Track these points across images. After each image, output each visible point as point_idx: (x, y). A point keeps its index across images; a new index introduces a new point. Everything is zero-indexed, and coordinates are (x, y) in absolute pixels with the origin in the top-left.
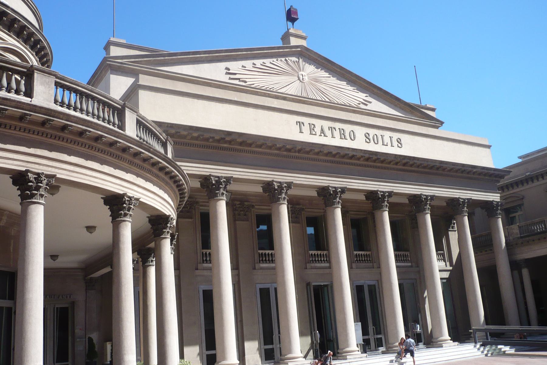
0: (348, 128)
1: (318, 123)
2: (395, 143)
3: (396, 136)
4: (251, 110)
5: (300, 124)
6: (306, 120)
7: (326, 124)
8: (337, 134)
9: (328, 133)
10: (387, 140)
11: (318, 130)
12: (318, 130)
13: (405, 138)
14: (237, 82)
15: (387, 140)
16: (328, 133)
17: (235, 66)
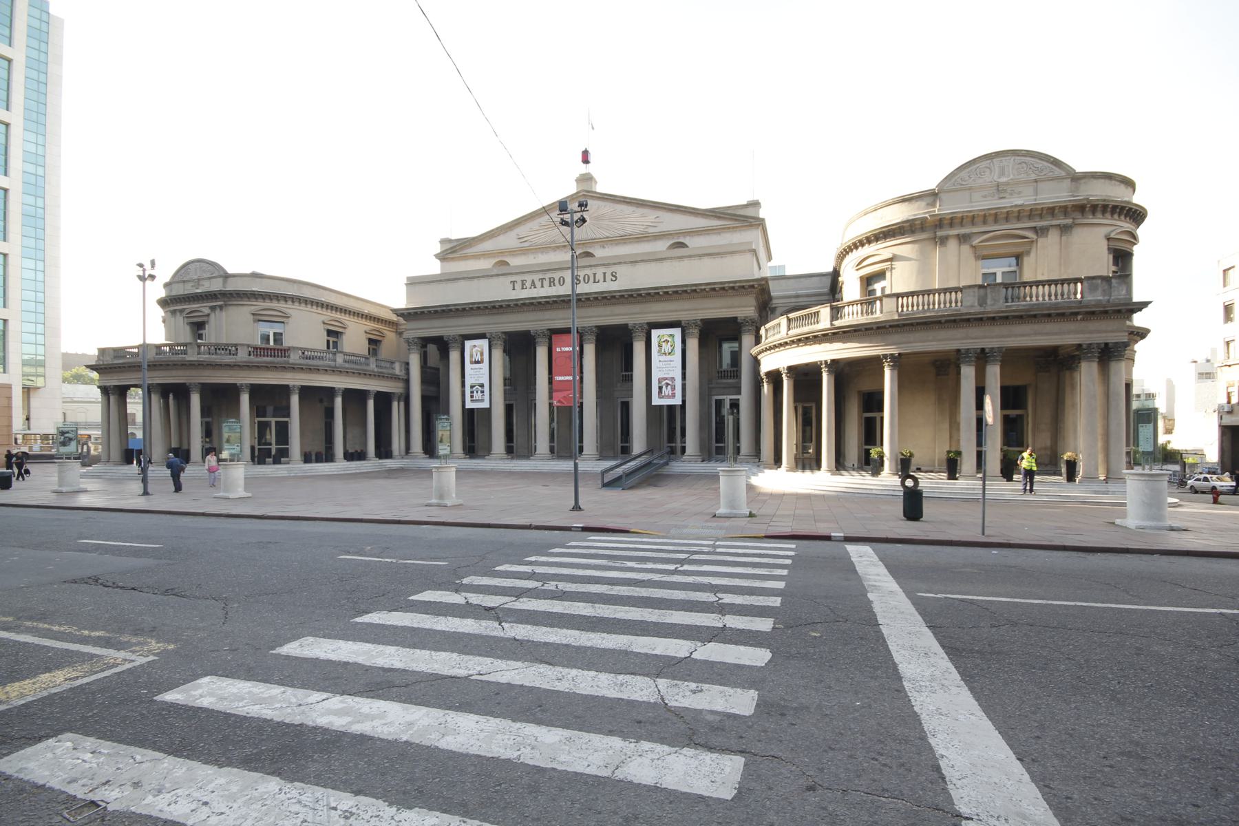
0: (557, 275)
1: (529, 278)
2: (609, 277)
3: (609, 271)
4: (476, 281)
5: (513, 282)
6: (518, 278)
7: (536, 277)
8: (546, 283)
9: (538, 284)
10: (600, 277)
11: (528, 284)
12: (528, 284)
13: (621, 270)
14: (526, 244)
15: (600, 277)
16: (538, 284)
17: (523, 230)
